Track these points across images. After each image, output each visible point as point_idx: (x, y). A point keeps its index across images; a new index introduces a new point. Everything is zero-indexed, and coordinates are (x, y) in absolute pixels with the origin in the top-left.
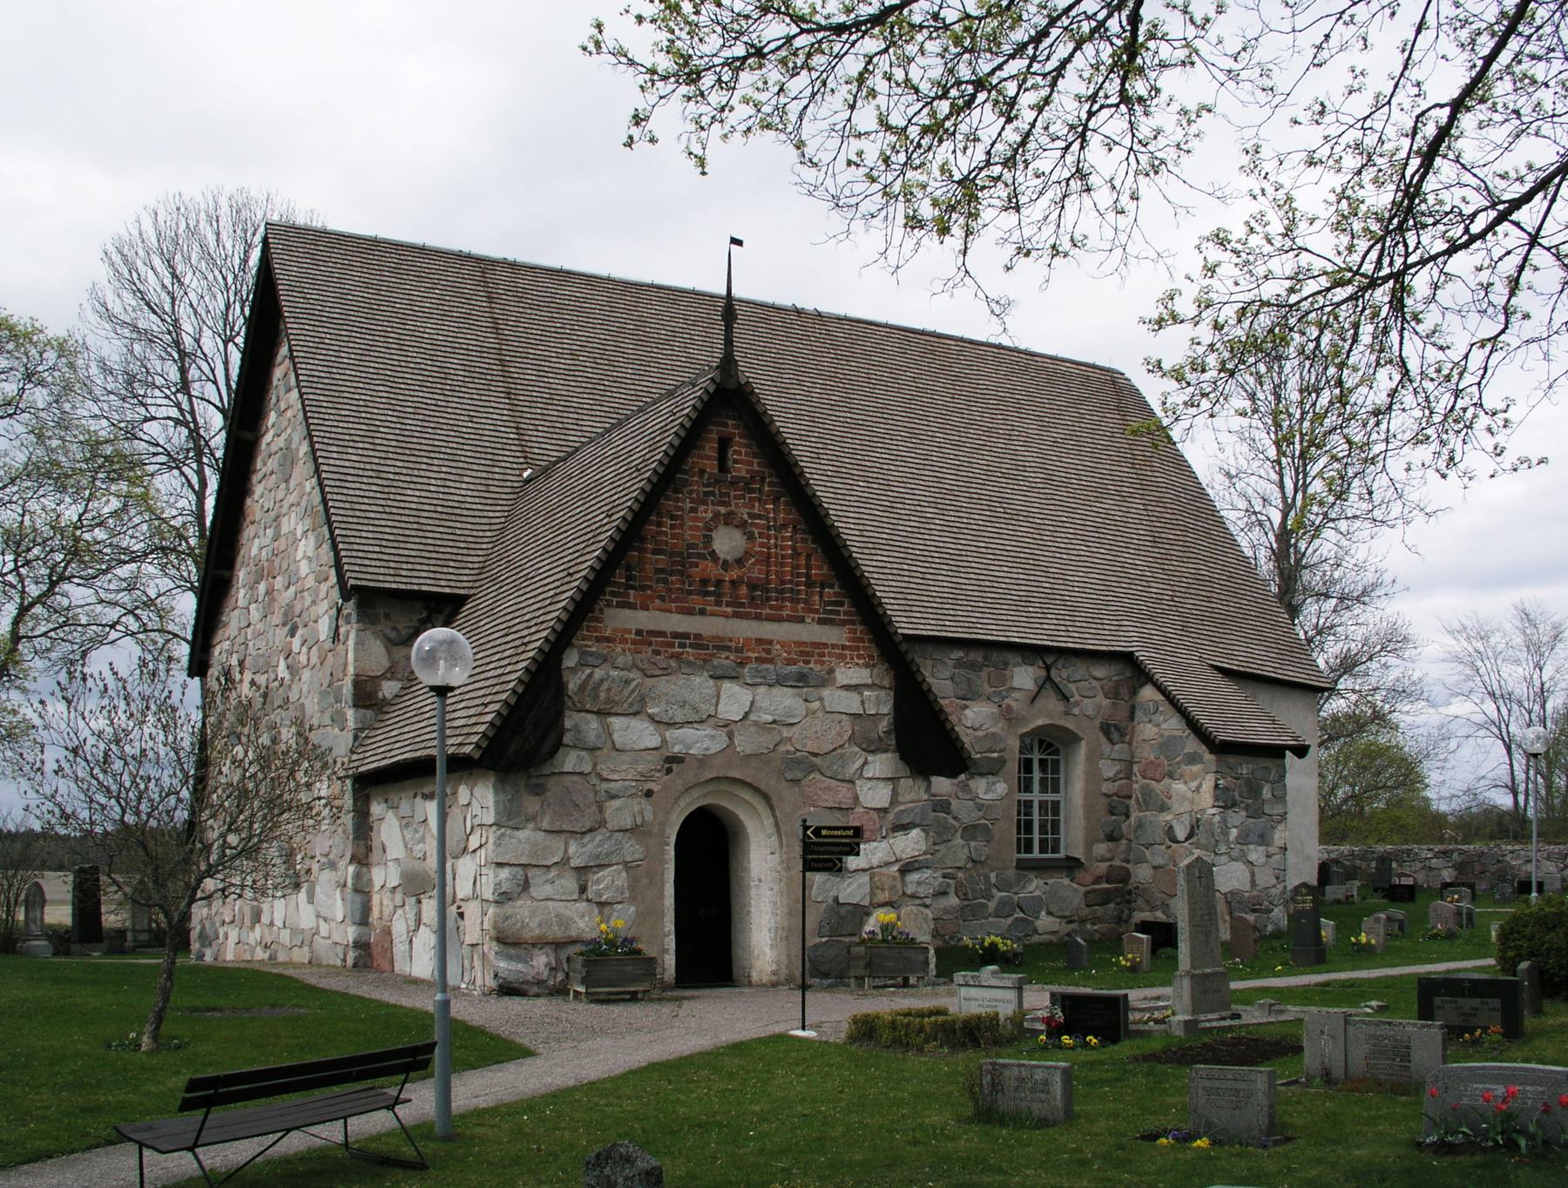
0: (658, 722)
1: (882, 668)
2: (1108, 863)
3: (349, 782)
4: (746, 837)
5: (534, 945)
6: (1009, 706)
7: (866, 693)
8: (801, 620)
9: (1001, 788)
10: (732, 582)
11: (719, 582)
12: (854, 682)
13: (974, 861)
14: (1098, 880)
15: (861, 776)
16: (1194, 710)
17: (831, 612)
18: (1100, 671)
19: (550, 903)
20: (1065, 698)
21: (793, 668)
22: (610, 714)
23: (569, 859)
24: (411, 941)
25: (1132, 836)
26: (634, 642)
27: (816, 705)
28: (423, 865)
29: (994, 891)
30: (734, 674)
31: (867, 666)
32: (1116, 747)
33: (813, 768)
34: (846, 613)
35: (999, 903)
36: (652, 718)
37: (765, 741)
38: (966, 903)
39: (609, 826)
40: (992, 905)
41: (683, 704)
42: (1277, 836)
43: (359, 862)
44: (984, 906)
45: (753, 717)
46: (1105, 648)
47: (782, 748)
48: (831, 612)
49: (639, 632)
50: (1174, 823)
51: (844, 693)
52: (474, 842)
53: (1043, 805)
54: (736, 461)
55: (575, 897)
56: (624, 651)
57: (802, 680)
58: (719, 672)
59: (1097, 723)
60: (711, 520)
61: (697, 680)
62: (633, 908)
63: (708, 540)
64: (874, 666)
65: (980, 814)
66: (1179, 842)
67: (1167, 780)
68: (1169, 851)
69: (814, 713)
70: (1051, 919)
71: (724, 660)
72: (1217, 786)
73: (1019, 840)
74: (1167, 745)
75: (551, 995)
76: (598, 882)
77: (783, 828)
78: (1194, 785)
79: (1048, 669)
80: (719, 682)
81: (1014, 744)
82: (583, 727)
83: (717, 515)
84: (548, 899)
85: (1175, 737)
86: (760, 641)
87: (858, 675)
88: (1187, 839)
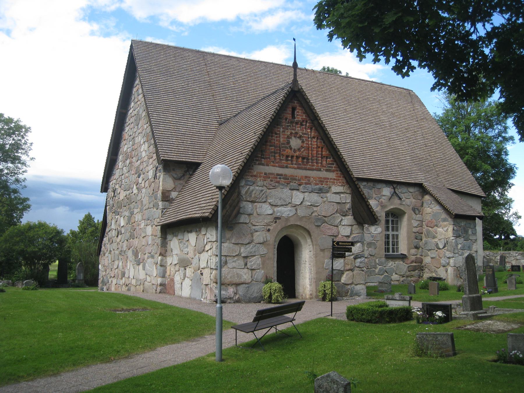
0: (272, 205)
1: (347, 187)
2: (416, 256)
3: (159, 227)
4: (301, 245)
5: (229, 285)
6: (382, 201)
7: (342, 195)
8: (320, 170)
9: (379, 230)
10: (297, 156)
11: (292, 157)
12: (337, 191)
13: (371, 255)
14: (412, 262)
15: (340, 224)
16: (444, 203)
17: (330, 167)
18: (411, 190)
19: (234, 269)
20: (400, 199)
21: (318, 186)
22: (255, 202)
23: (241, 254)
24: (182, 283)
25: (423, 247)
26: (264, 177)
27: (325, 199)
28: (187, 256)
29: (378, 266)
30: (298, 188)
31: (342, 186)
32: (417, 216)
33: (325, 222)
34: (335, 167)
35: (379, 270)
36: (270, 203)
37: (309, 211)
38: (368, 270)
39: (255, 242)
40: (377, 271)
41: (280, 199)
42: (473, 247)
43: (163, 255)
44: (374, 271)
45: (304, 203)
46: (413, 182)
47: (314, 214)
48: (330, 167)
49: (265, 174)
50: (439, 242)
51: (334, 195)
52: (207, 248)
53: (393, 235)
54: (297, 115)
55: (243, 267)
56: (260, 180)
57: (320, 191)
58: (292, 188)
59: (411, 207)
60: (289, 135)
61: (285, 190)
62: (263, 271)
63: (288, 143)
64: (344, 186)
65: (372, 239)
66: (440, 249)
67: (435, 228)
68: (437, 252)
69: (324, 202)
70: (397, 276)
71: (294, 184)
72: (454, 229)
73: (385, 248)
74: (435, 215)
75: (234, 302)
76: (251, 262)
78: (445, 229)
79: (394, 188)
80: (292, 191)
81: (384, 214)
82: (246, 206)
83: (291, 133)
84: (234, 268)
85: (438, 212)
86: (306, 177)
87: (340, 189)
88: (443, 248)
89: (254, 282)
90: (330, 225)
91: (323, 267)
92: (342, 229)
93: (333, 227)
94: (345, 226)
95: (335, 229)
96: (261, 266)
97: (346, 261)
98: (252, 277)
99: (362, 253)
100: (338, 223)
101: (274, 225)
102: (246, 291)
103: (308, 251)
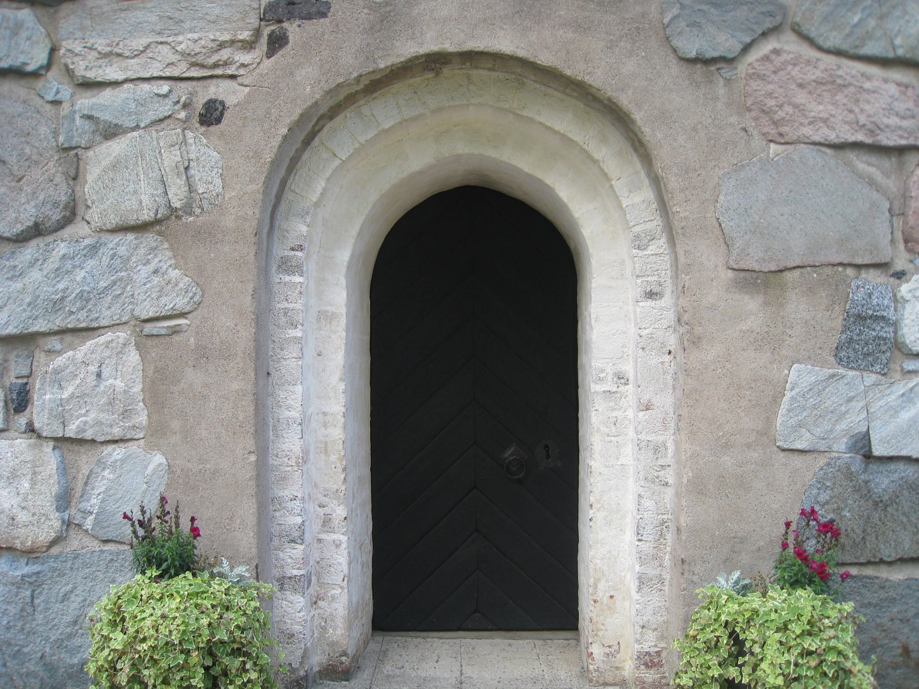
39: (94, 215)
77: (681, 210)
89: (75, 542)
90: (839, 53)
91: (766, 433)
95: (893, 89)
96: (142, 418)
98: (64, 500)
101: (268, 63)
102: (13, 610)
103: (633, 289)
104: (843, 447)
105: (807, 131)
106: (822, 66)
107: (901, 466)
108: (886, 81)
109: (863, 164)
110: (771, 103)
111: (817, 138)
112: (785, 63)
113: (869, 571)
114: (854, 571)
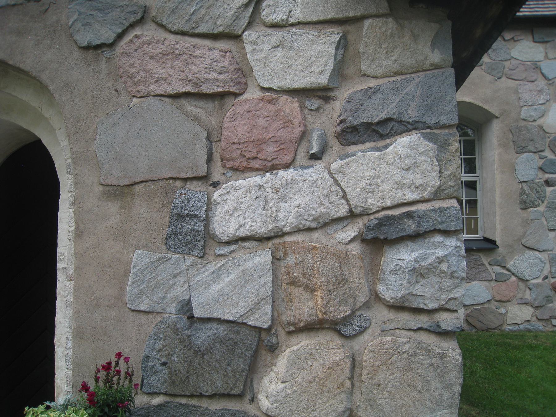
90: (183, 33)
91: (120, 297)
92: (266, 47)
93: (207, 43)
94: (294, 30)
95: (215, 54)
97: (291, 260)
99: (438, 204)
100: (237, 17)
104: (173, 310)
105: (153, 87)
106: (167, 42)
107: (215, 325)
108: (210, 49)
109: (190, 106)
110: (133, 70)
111: (159, 92)
112: (144, 43)
113: (194, 402)
114: (183, 401)
